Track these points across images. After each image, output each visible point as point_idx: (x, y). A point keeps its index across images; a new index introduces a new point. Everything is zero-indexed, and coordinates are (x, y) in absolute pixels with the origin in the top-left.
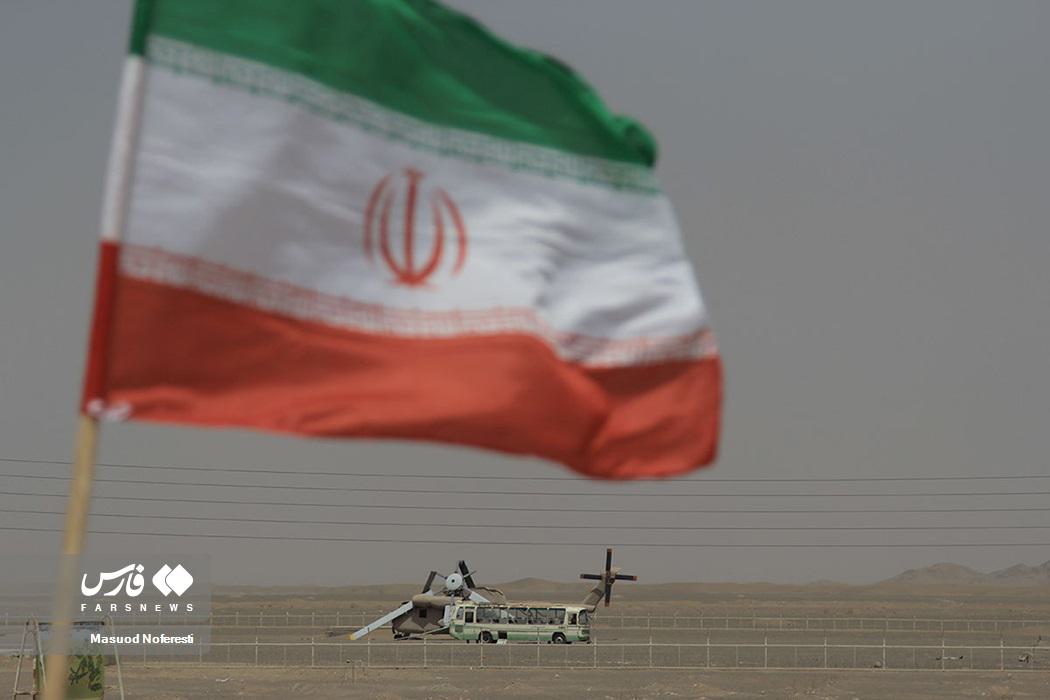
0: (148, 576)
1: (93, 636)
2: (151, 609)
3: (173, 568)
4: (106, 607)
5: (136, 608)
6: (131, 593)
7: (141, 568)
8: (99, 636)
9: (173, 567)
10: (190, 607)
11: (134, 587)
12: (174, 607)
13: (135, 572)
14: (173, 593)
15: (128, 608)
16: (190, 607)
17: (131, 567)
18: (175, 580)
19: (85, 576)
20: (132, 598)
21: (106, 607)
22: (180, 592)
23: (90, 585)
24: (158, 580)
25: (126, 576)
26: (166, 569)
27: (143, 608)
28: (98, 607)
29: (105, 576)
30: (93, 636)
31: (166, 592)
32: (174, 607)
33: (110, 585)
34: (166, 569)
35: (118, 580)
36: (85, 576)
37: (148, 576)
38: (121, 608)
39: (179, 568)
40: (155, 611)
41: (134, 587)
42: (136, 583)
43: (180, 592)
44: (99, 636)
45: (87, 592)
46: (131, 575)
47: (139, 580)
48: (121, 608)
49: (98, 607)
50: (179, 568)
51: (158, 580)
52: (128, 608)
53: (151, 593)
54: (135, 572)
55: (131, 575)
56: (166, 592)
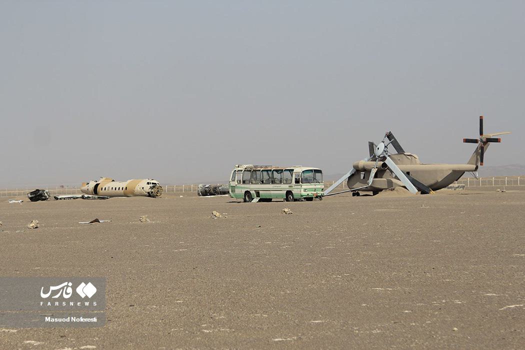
0: (74, 288)
1: (46, 318)
4: (53, 304)
5: (68, 303)
6: (66, 296)
8: (49, 318)
9: (86, 283)
10: (95, 304)
11: (67, 294)
12: (87, 304)
13: (67, 286)
14: (86, 297)
15: (64, 304)
16: (95, 304)
17: (66, 284)
18: (88, 290)
19: (43, 288)
23: (45, 293)
24: (79, 290)
25: (63, 288)
26: (83, 284)
27: (72, 304)
28: (49, 304)
29: (52, 288)
31: (83, 296)
32: (87, 304)
33: (55, 292)
34: (83, 284)
36: (43, 288)
37: (74, 288)
38: (61, 304)
39: (90, 284)
40: (78, 305)
41: (67, 294)
42: (68, 292)
44: (49, 318)
45: (44, 296)
46: (65, 288)
47: (70, 290)
48: (61, 304)
49: (49, 304)
50: (90, 284)
51: (79, 290)
52: (64, 304)
53: (75, 296)
54: (67, 286)
55: (65, 288)
56: (83, 296)
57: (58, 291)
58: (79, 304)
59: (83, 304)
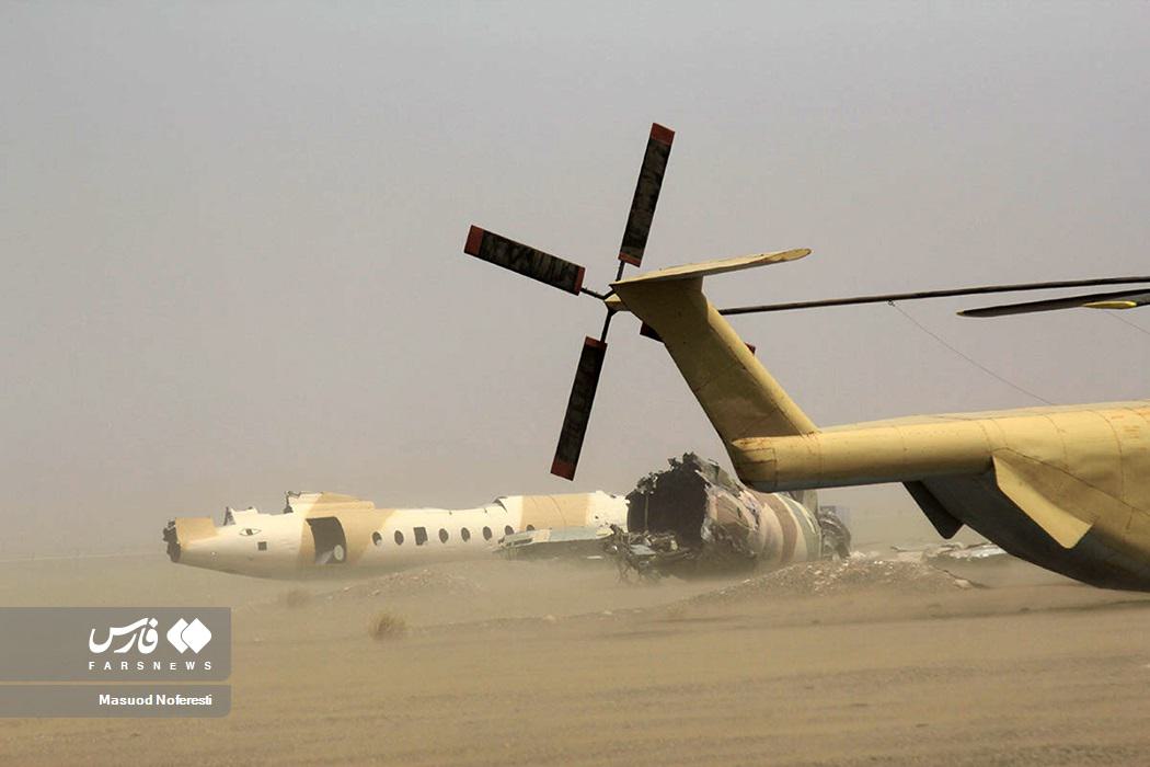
0: (162, 631)
1: (101, 696)
2: (165, 666)
3: (189, 622)
4: (116, 665)
5: (148, 664)
6: (144, 650)
7: (154, 623)
8: (108, 696)
9: (189, 622)
10: (208, 666)
12: (190, 666)
13: (148, 627)
14: (189, 650)
15: (140, 666)
16: (208, 666)
17: (144, 622)
19: (93, 631)
20: (145, 655)
21: (116, 665)
22: (197, 649)
23: (99, 641)
24: (173, 636)
25: (138, 631)
26: (182, 623)
27: (157, 666)
28: (108, 665)
29: (115, 631)
30: (101, 696)
31: (182, 649)
32: (190, 666)
33: (120, 641)
34: (182, 623)
35: (129, 636)
36: (93, 631)
37: (162, 631)
38: (132, 665)
39: (197, 622)
41: (146, 643)
42: (149, 639)
43: (197, 649)
44: (108, 696)
45: (96, 648)
47: (153, 636)
48: (132, 665)
49: (108, 665)
50: (197, 622)
51: (173, 636)
52: (140, 666)
53: (165, 649)
54: (148, 627)
56: (182, 649)
57: (127, 637)
58: (172, 666)
59: (181, 666)
